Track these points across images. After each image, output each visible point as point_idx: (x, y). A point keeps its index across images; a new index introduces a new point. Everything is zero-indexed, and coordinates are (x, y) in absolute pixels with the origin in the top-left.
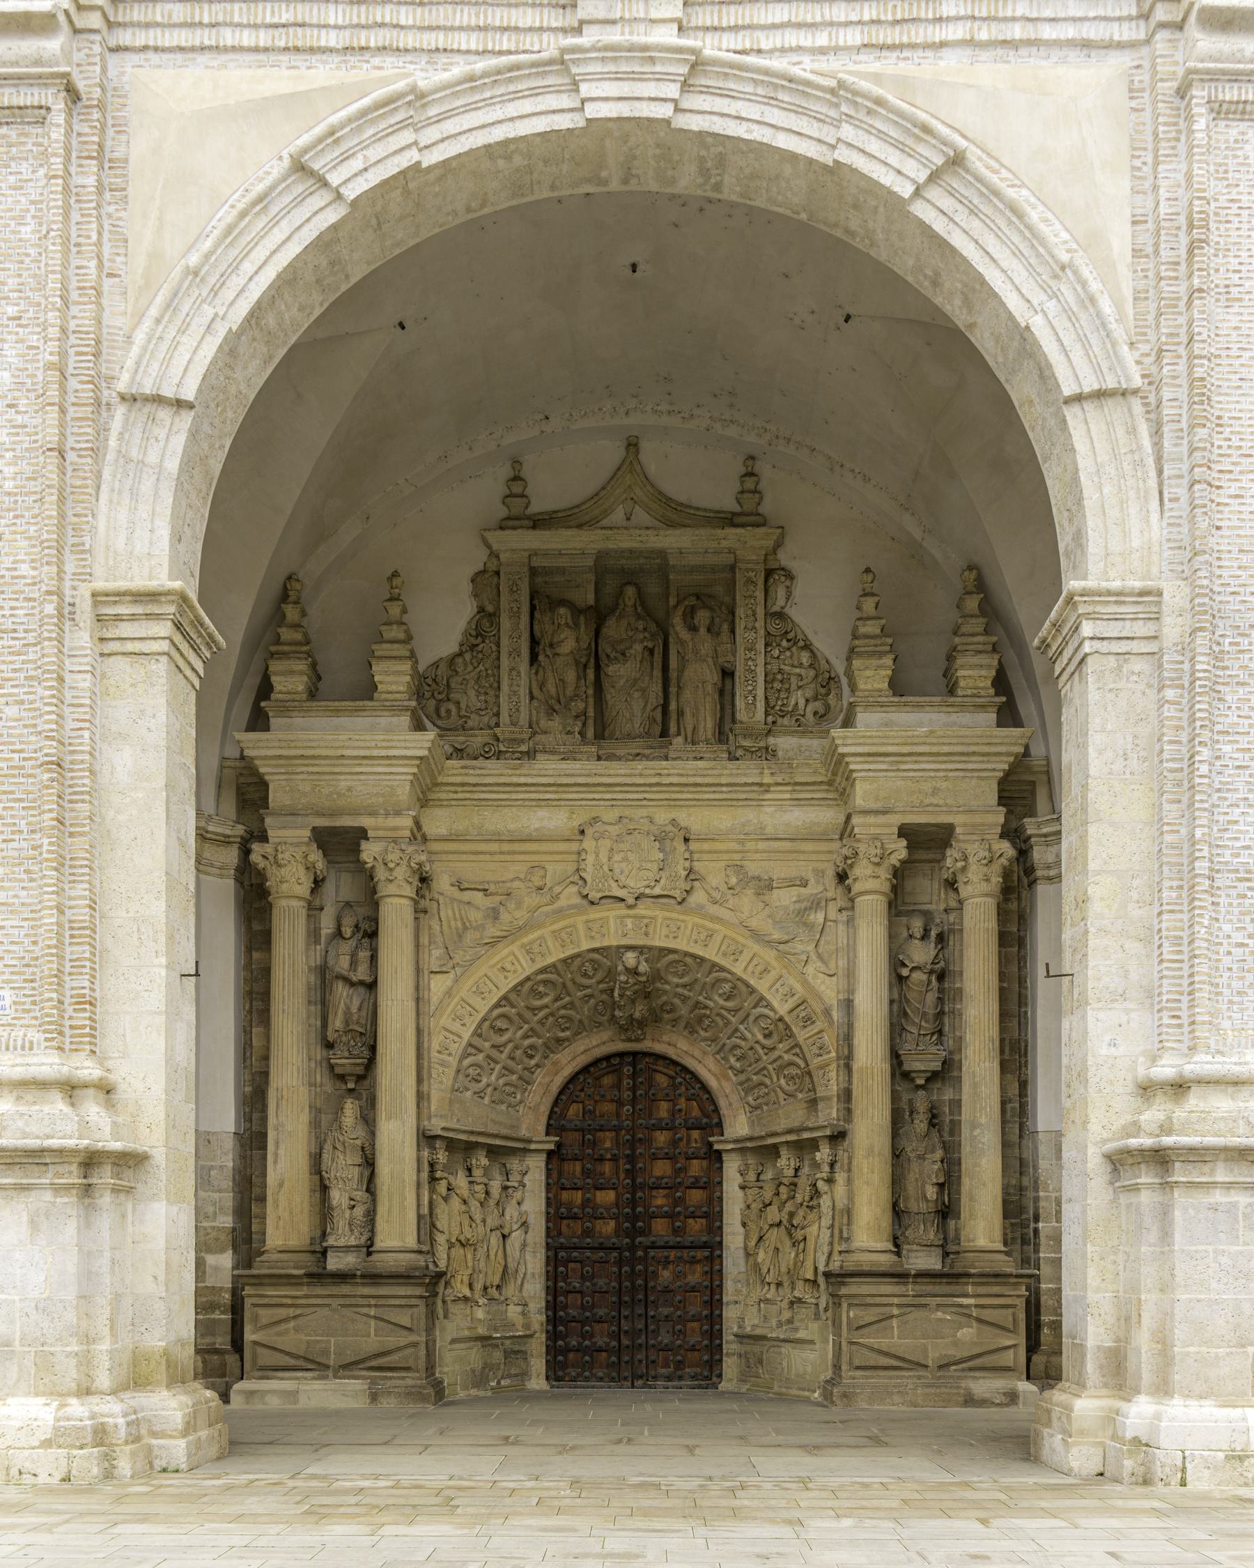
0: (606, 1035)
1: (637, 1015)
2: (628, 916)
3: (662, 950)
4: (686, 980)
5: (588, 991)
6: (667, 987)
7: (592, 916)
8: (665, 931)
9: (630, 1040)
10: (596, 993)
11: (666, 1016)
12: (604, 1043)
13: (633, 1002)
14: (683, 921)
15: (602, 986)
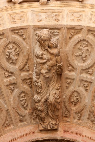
0: (28, 129)
1: (51, 99)
2: (43, 11)
3: (69, 28)
4: (89, 62)
5: (12, 79)
6: (73, 74)
7: (14, 11)
8: (70, 17)
9: (46, 130)
10: (19, 82)
11: (74, 109)
12: (27, 135)
13: (48, 80)
14: (84, 12)
15: (24, 74)
